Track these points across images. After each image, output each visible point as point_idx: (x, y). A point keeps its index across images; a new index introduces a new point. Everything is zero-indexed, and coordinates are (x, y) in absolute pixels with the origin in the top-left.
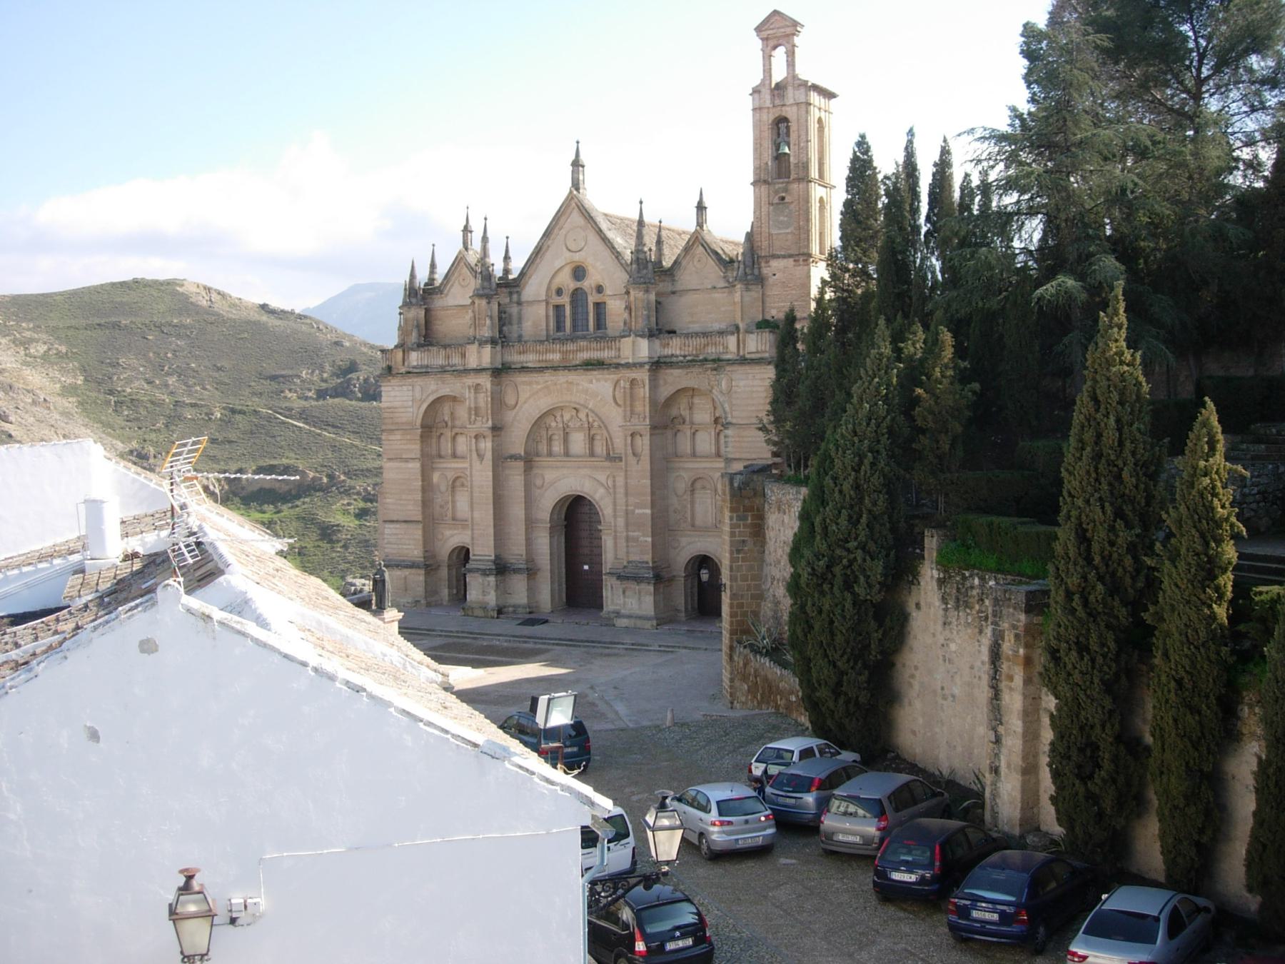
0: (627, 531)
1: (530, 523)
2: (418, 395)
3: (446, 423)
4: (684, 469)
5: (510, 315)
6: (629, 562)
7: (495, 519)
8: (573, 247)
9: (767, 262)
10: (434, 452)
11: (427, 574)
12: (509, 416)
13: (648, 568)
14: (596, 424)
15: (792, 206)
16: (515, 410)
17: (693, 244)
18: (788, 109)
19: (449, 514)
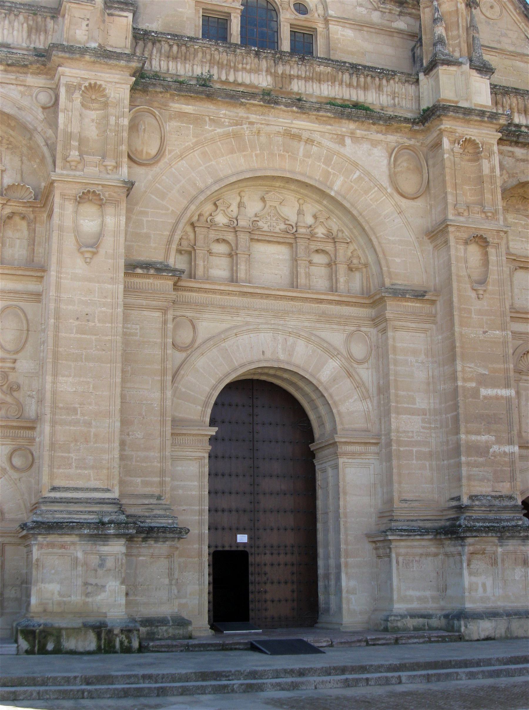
14: (320, 231)
16: (156, 169)
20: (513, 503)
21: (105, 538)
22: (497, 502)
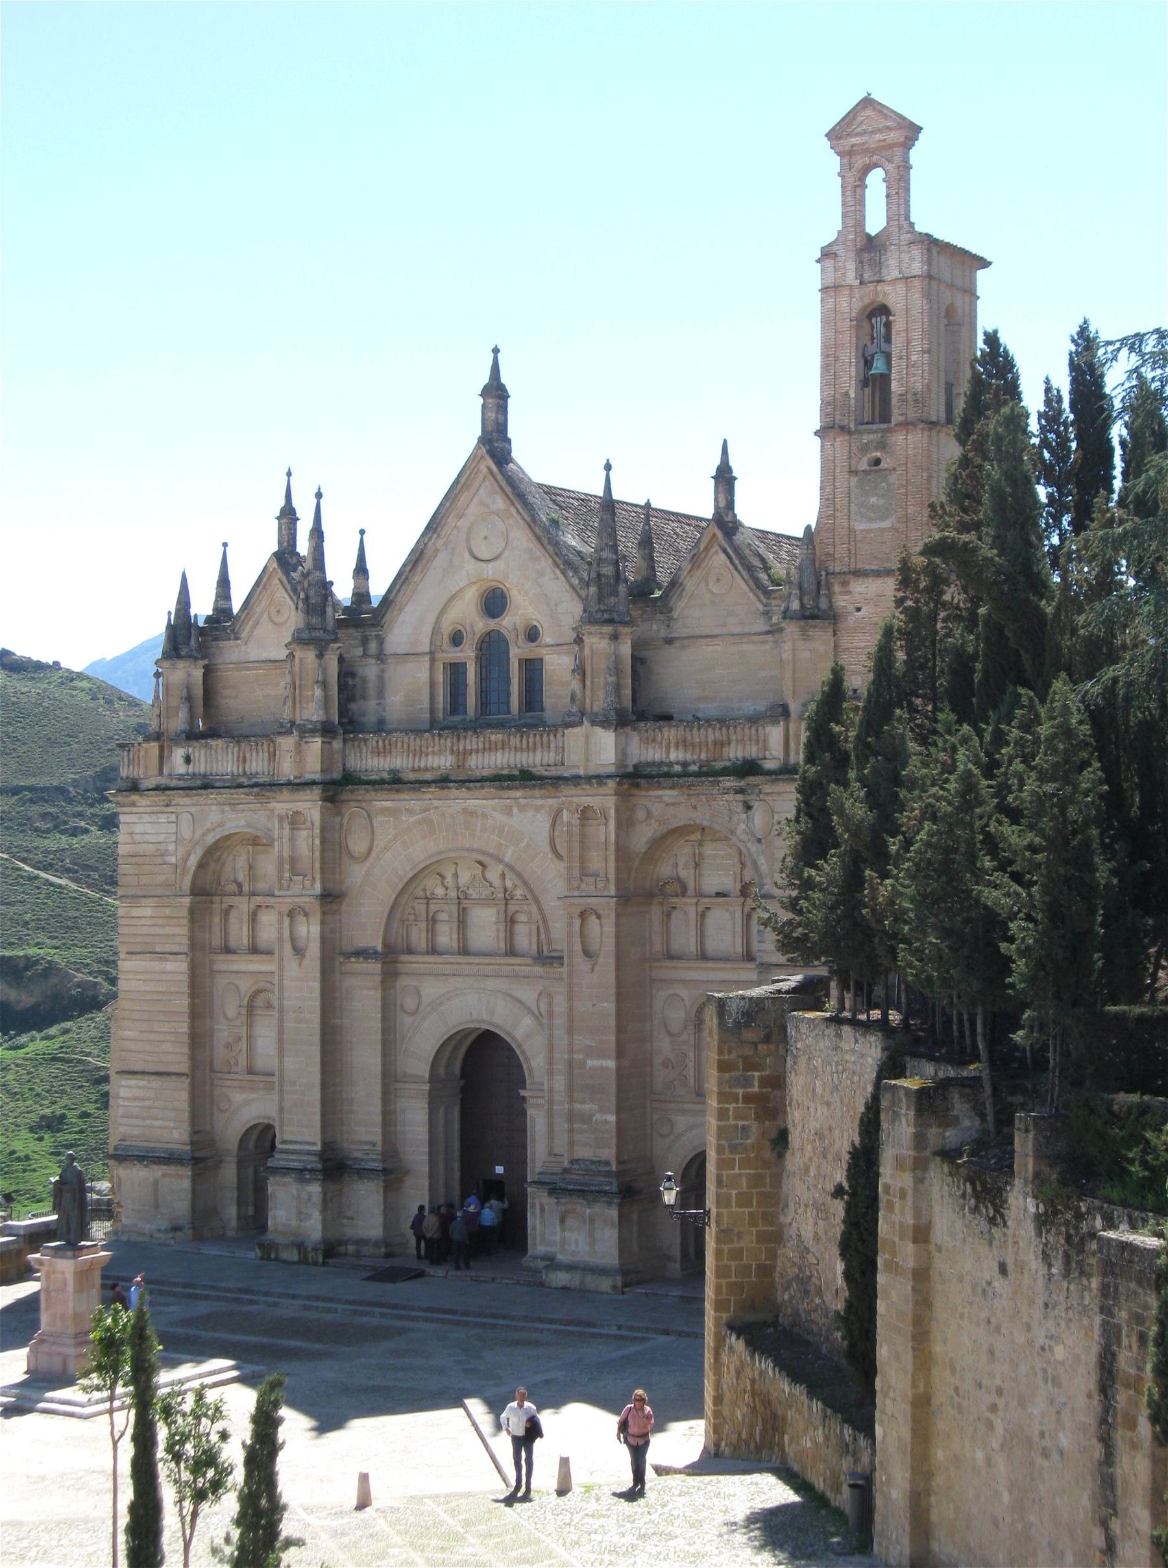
0: (571, 1100)
1: (390, 1080)
2: (186, 832)
3: (240, 886)
4: (683, 982)
5: (364, 681)
6: (573, 1162)
7: (324, 1072)
8: (484, 553)
9: (845, 584)
10: (217, 941)
11: (196, 1178)
12: (355, 874)
13: (609, 1174)
14: (518, 893)
15: (893, 478)
16: (367, 864)
17: (707, 549)
18: (887, 288)
19: (243, 1062)
20: (607, 1169)
21: (308, 1181)
22: (593, 1167)
